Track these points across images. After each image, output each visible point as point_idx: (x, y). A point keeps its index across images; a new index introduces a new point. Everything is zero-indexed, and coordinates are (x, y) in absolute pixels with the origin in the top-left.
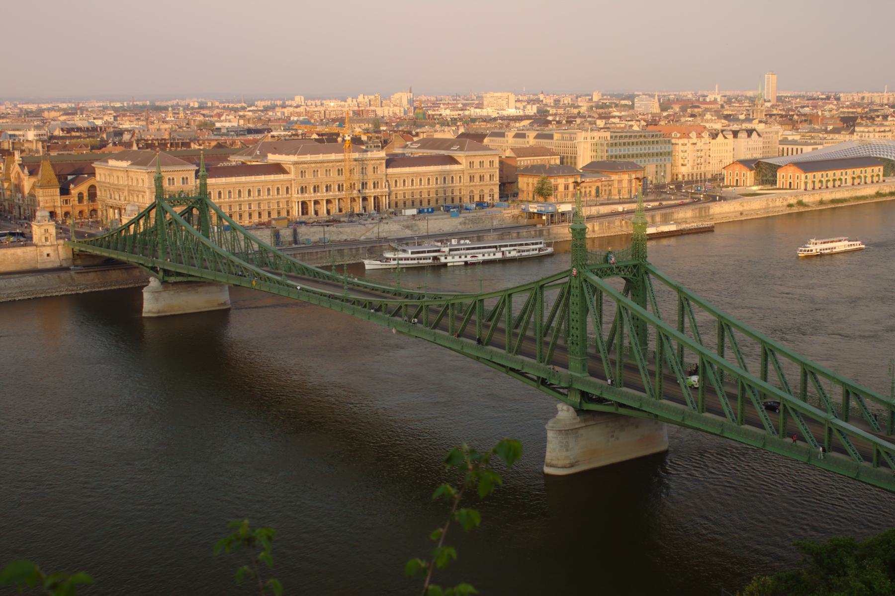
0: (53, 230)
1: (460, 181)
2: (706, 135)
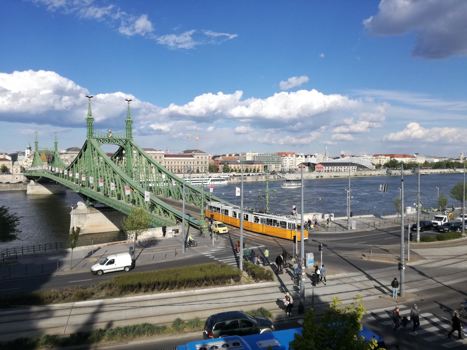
1: (194, 164)
2: (294, 156)
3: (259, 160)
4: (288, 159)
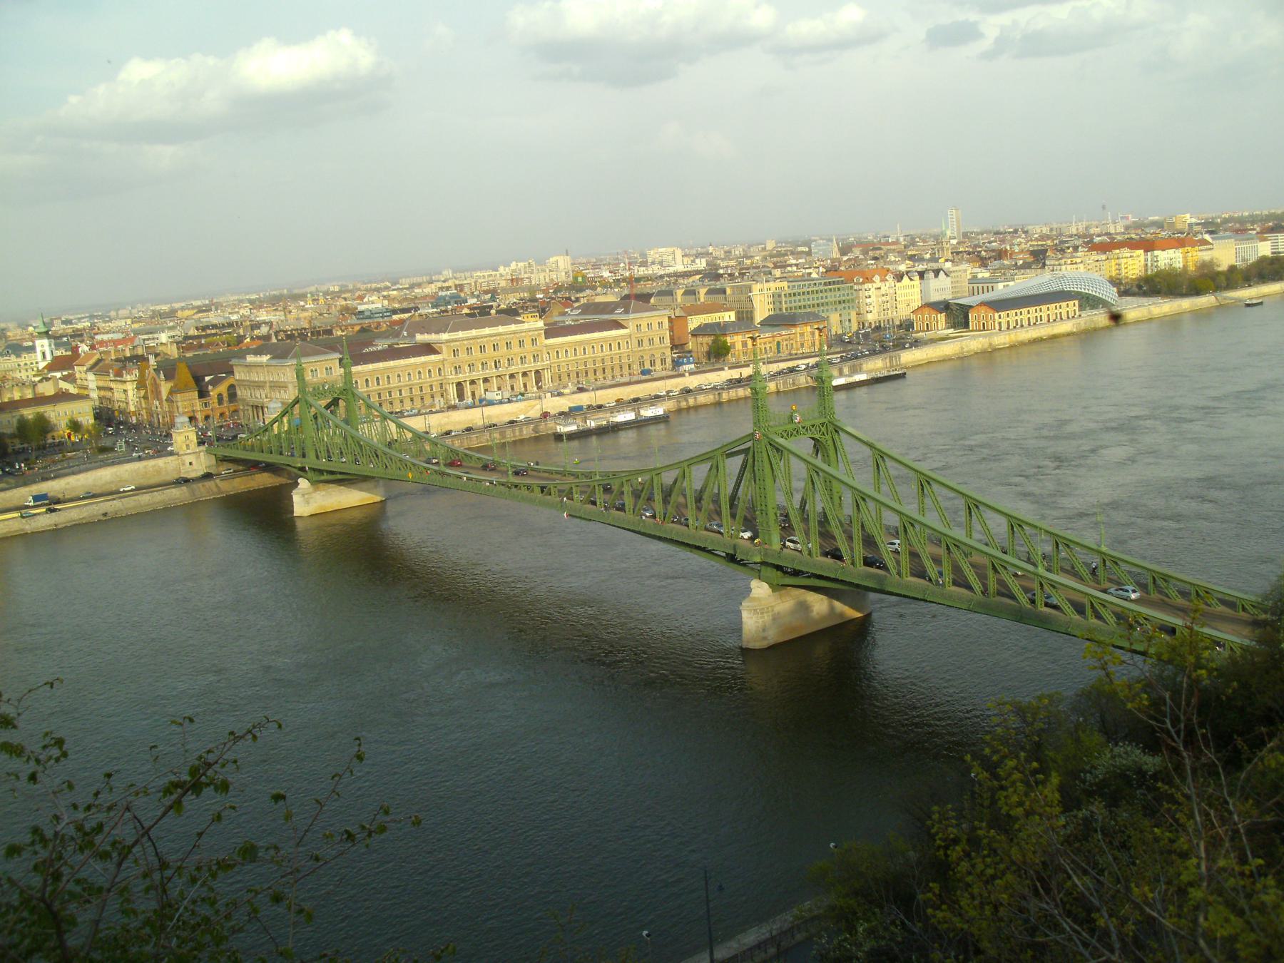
0: (193, 437)
2: (890, 277)
3: (809, 310)
4: (873, 292)
